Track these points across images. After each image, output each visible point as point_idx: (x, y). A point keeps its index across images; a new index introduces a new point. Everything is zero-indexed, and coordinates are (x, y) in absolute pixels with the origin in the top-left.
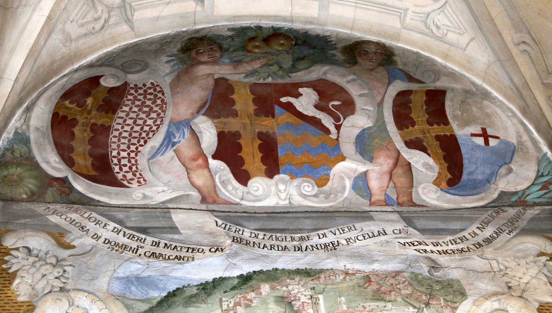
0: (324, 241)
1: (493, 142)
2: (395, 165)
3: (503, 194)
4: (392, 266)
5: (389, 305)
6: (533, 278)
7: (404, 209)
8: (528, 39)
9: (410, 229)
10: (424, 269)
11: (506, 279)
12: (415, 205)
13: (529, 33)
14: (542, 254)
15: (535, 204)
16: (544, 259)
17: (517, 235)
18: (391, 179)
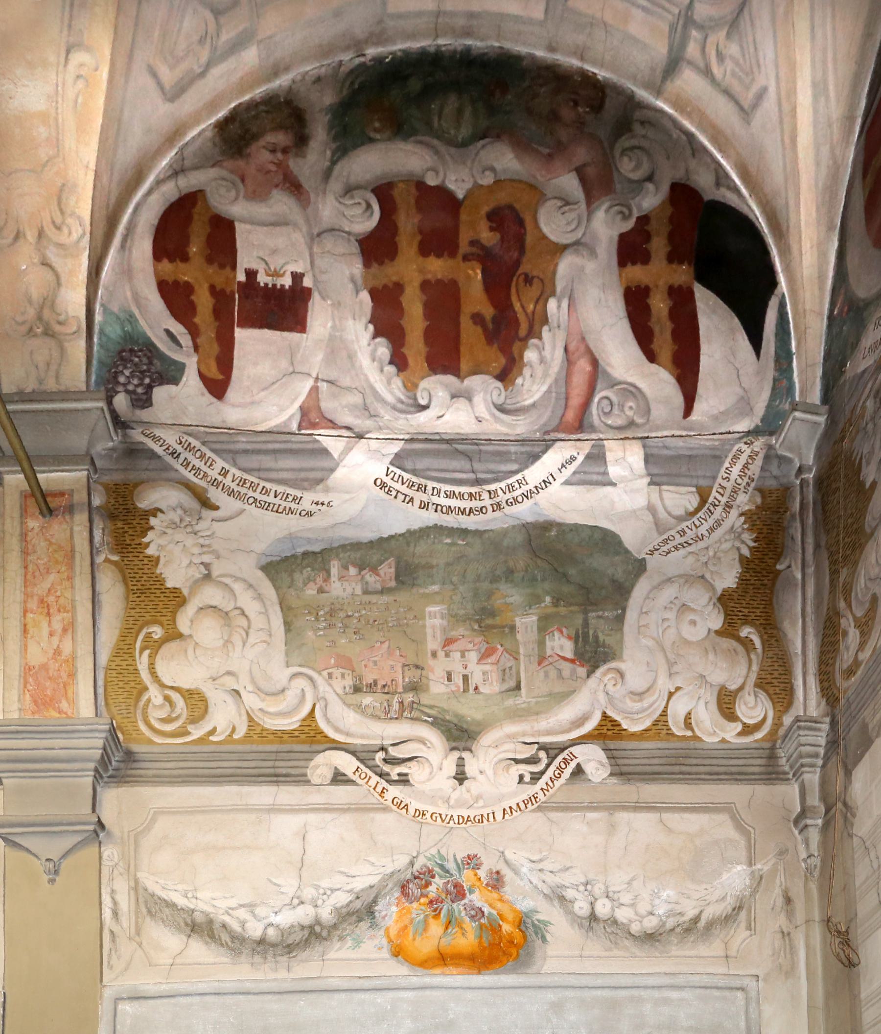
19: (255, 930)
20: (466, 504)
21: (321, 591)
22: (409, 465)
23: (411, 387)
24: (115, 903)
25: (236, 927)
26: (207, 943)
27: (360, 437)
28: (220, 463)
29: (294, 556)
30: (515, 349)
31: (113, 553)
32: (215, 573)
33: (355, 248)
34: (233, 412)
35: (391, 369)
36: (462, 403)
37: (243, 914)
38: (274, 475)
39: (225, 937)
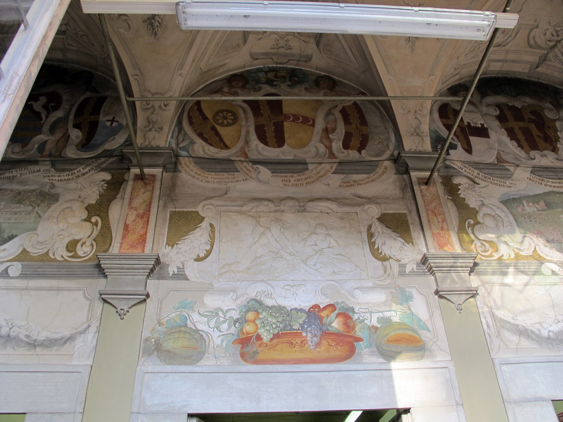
0: (11, 175)
1: (115, 124)
2: (62, 137)
3: (105, 151)
4: (32, 188)
5: (22, 206)
6: (93, 192)
7: (55, 159)
8: (138, 72)
9: (53, 169)
10: (46, 189)
11: (80, 193)
12: (61, 157)
13: (139, 70)
14: (104, 180)
15: (116, 156)
16: (104, 182)
17: (99, 171)
18: (57, 144)
19: (545, 333)
20: (558, 185)
21: (523, 210)
22: (536, 173)
23: (527, 153)
24: (487, 322)
25: (537, 332)
26: (527, 339)
27: (518, 166)
28: (476, 172)
29: (510, 199)
30: (554, 144)
31: (450, 196)
32: (485, 203)
33: (496, 119)
34: (475, 158)
35: (519, 148)
36: (544, 158)
37: (537, 326)
38: (495, 175)
39: (534, 336)
